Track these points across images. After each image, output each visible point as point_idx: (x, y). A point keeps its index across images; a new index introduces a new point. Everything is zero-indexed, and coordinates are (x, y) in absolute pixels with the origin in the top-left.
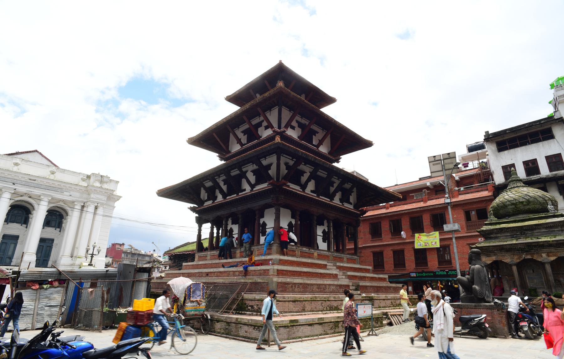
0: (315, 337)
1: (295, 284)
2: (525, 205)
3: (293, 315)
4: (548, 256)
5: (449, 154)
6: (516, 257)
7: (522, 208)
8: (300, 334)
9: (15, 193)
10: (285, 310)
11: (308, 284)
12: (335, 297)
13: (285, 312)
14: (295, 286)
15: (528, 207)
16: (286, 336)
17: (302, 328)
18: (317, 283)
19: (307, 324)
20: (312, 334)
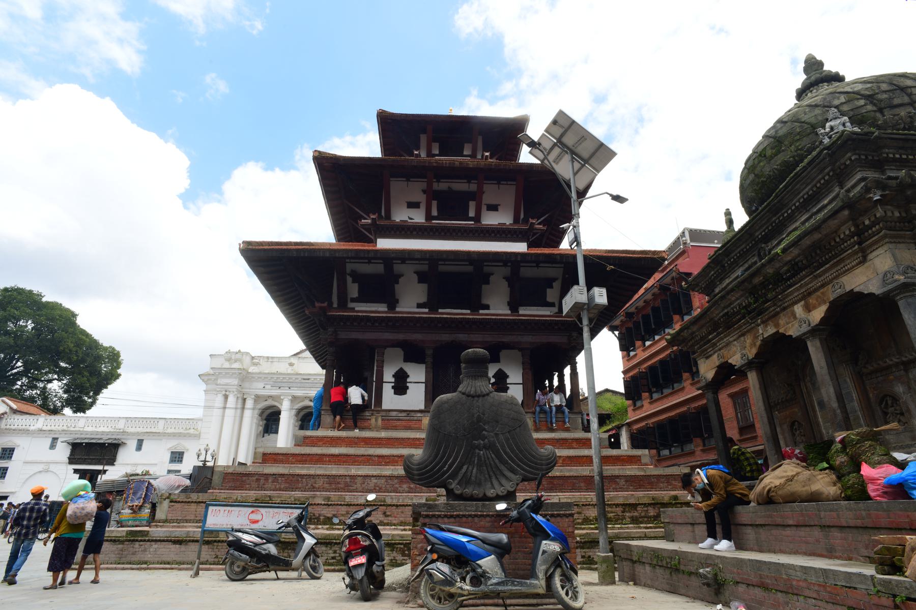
0: (185, 566)
1: (267, 476)
2: (772, 157)
3: (178, 527)
4: (808, 309)
5: (555, 122)
6: (748, 340)
7: (767, 170)
8: (148, 557)
9: (294, 399)
10: (188, 518)
11: (302, 476)
12: (328, 499)
13: (187, 521)
14: (267, 480)
15: (781, 158)
16: (113, 557)
17: (155, 546)
18: (328, 473)
19: (167, 541)
20: (178, 559)
